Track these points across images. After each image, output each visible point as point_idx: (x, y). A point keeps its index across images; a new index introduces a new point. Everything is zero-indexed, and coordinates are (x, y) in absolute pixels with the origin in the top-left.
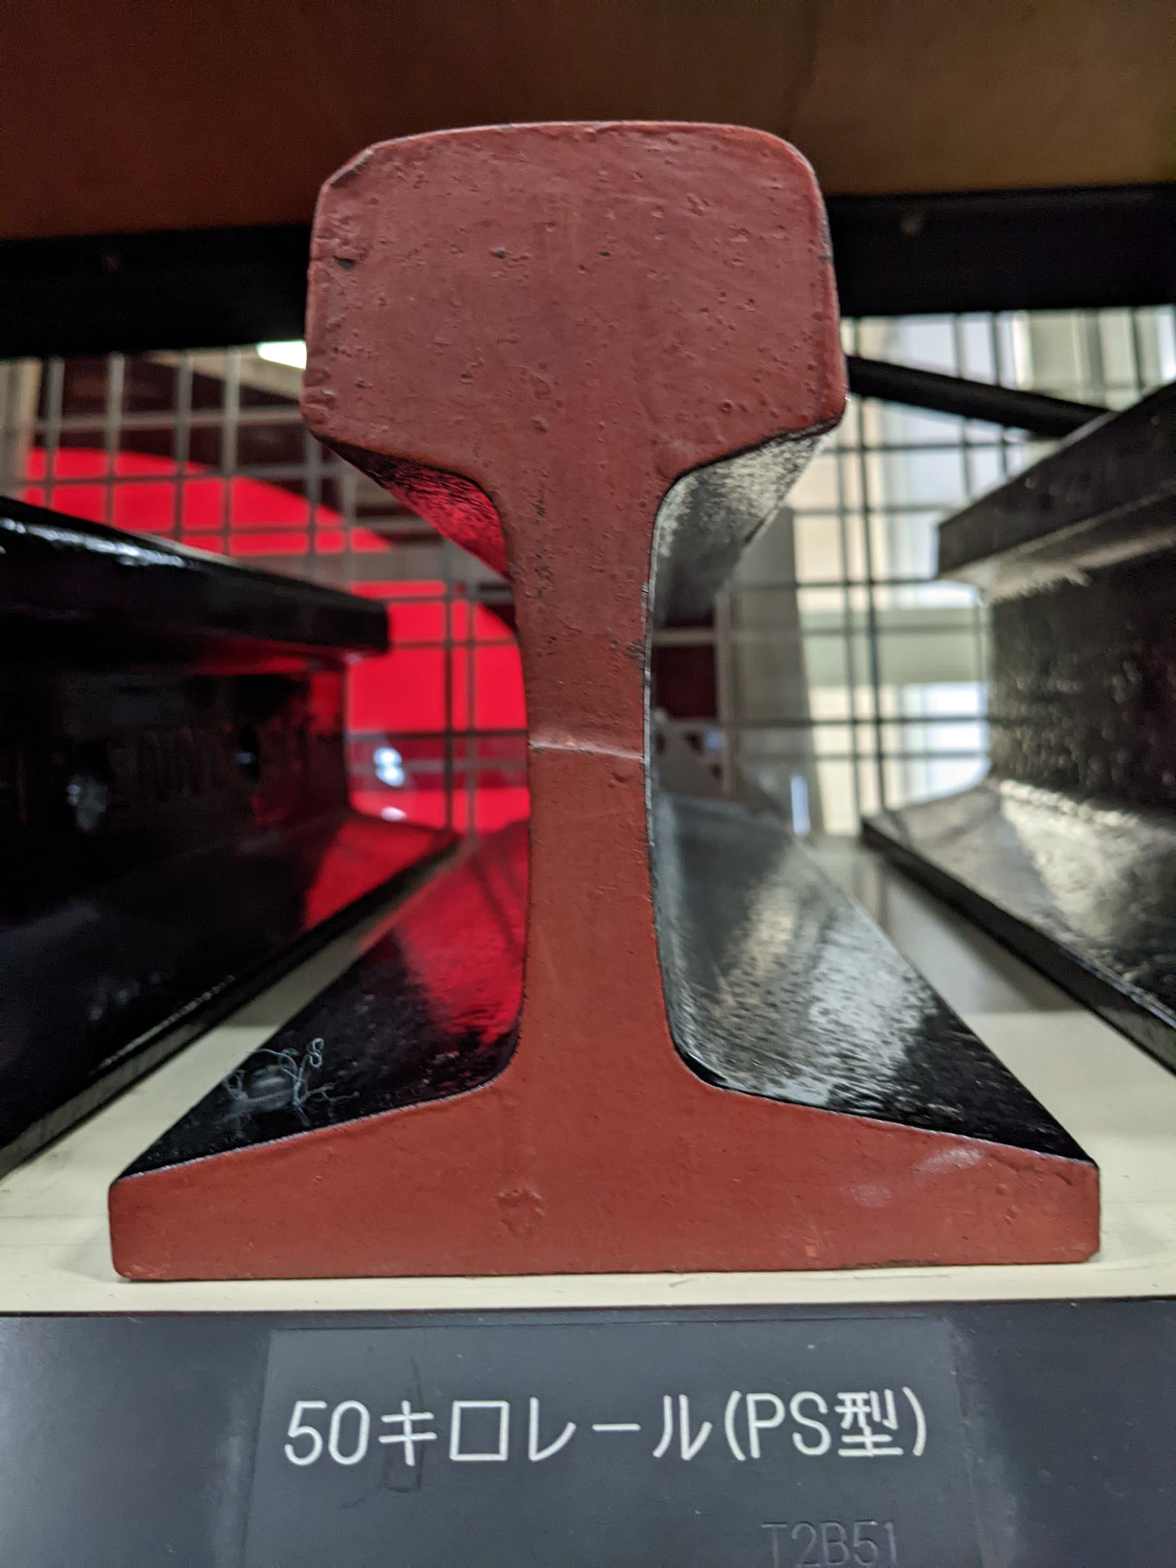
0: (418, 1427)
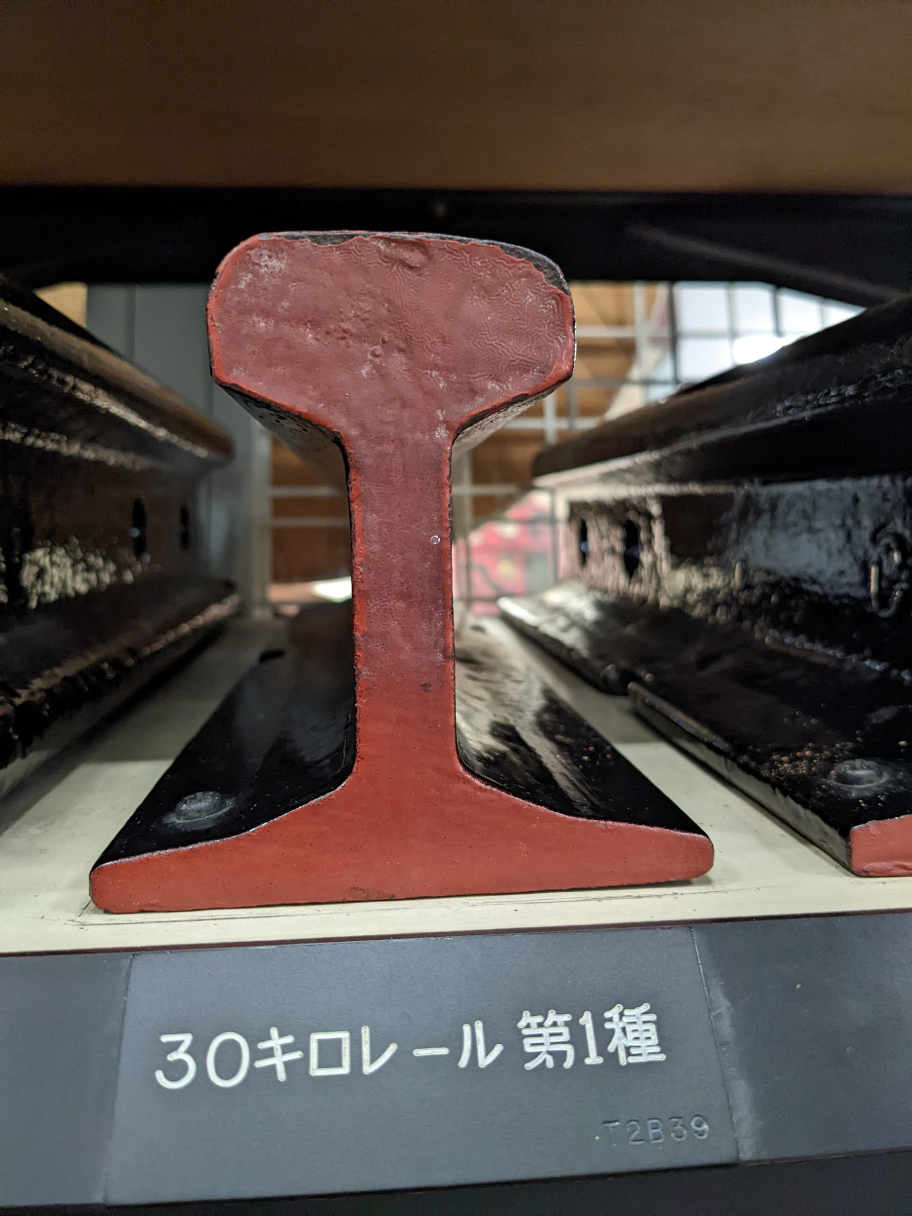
0: (286, 1049)
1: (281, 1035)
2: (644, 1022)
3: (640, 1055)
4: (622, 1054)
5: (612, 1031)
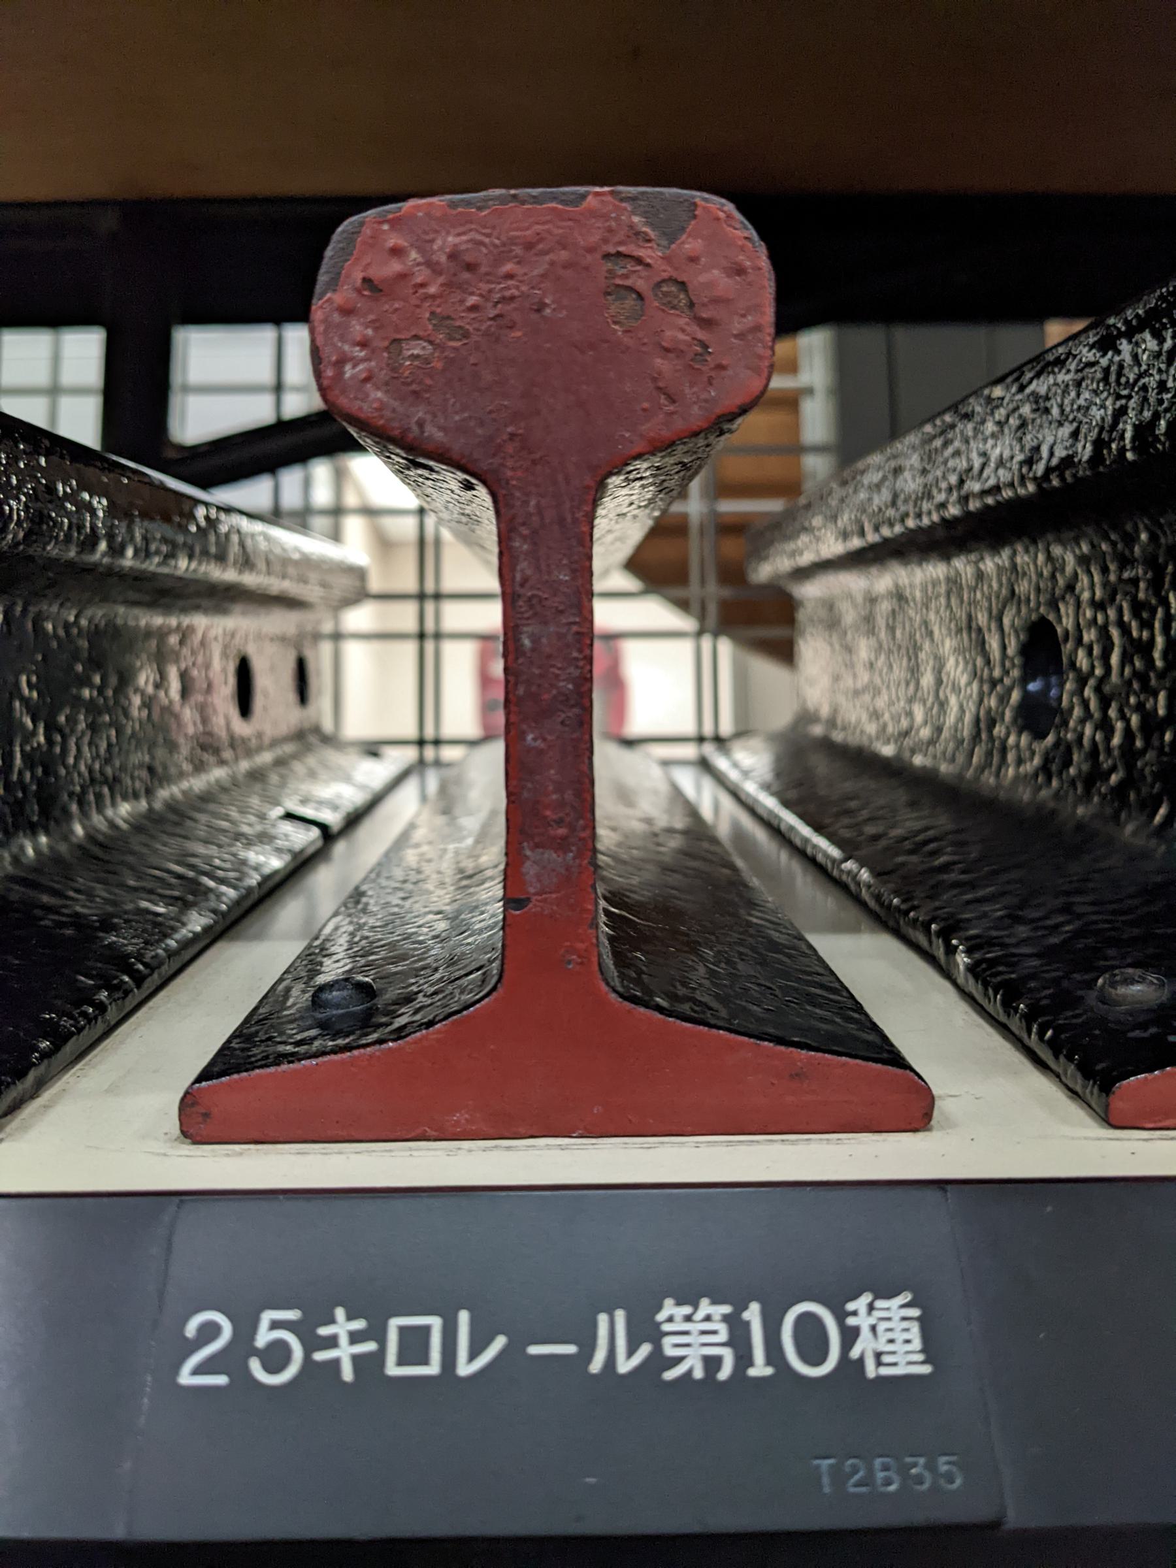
0: (355, 1337)
1: (350, 1317)
2: (904, 1319)
3: (895, 1364)
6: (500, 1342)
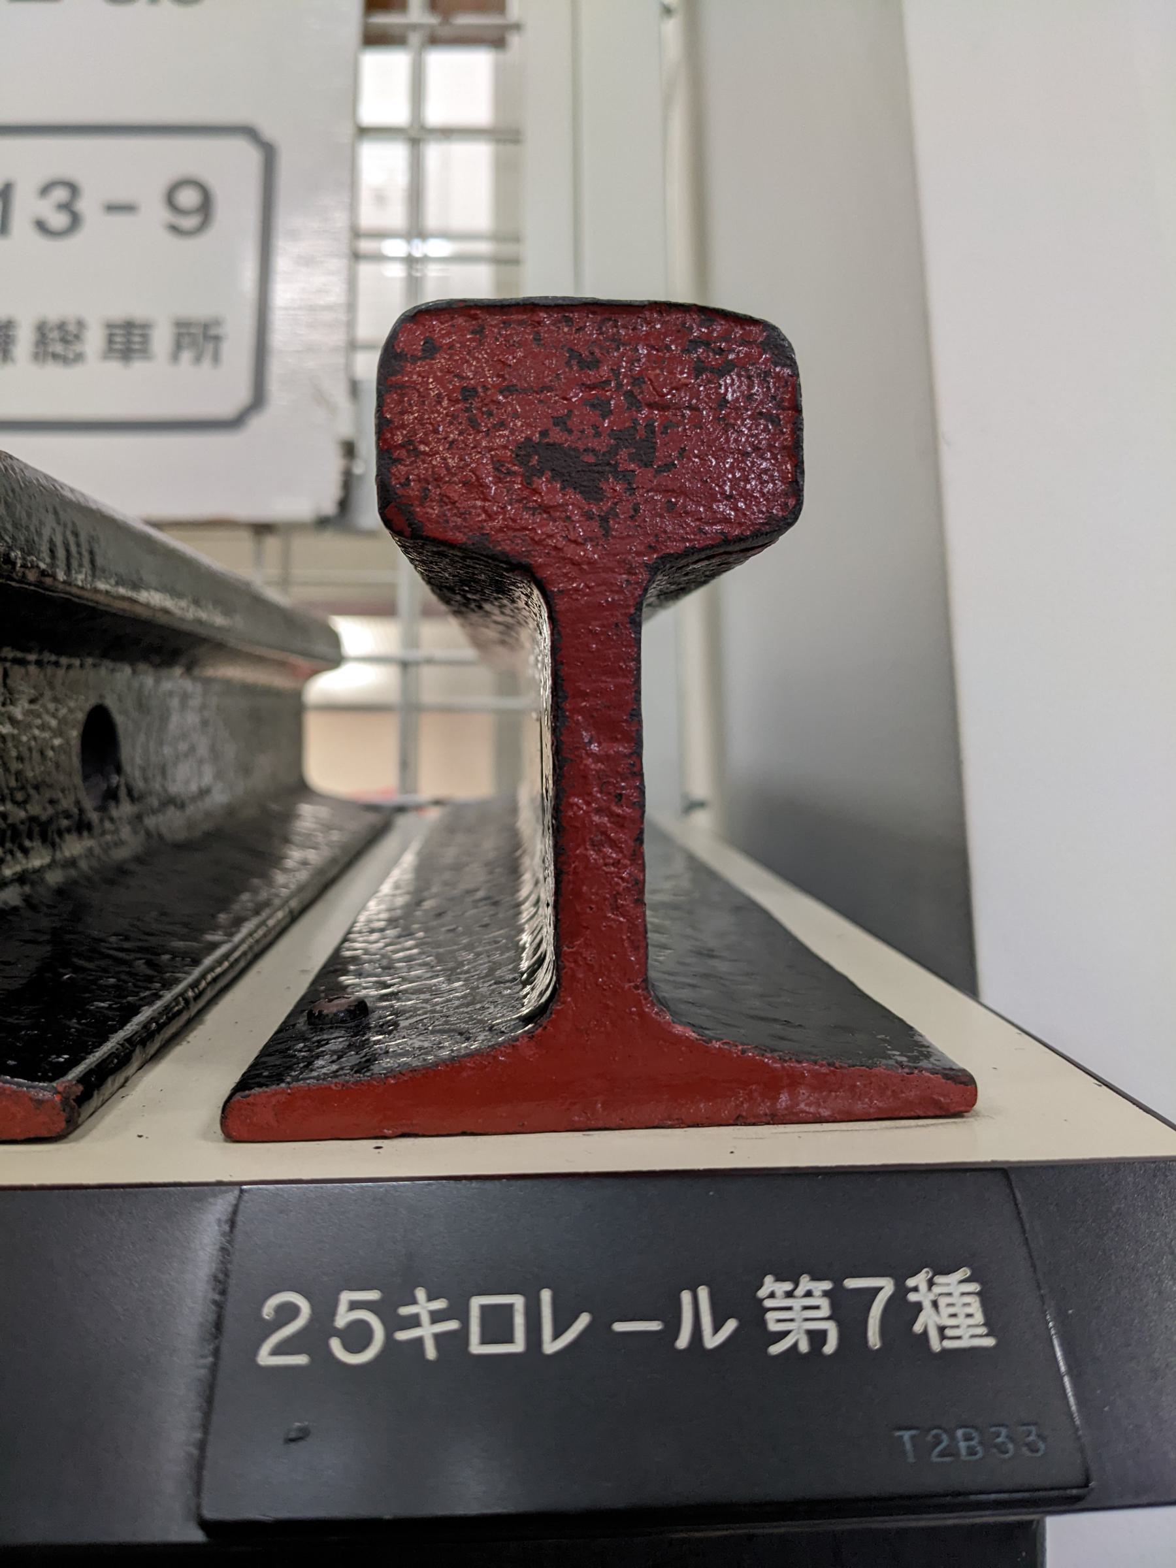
0: (436, 1317)
3: (959, 1338)
4: (933, 1335)
5: (918, 1307)
6: (584, 1320)
